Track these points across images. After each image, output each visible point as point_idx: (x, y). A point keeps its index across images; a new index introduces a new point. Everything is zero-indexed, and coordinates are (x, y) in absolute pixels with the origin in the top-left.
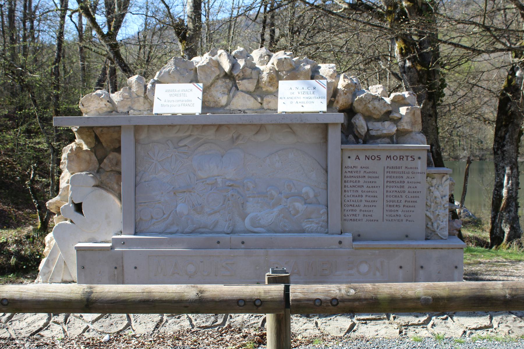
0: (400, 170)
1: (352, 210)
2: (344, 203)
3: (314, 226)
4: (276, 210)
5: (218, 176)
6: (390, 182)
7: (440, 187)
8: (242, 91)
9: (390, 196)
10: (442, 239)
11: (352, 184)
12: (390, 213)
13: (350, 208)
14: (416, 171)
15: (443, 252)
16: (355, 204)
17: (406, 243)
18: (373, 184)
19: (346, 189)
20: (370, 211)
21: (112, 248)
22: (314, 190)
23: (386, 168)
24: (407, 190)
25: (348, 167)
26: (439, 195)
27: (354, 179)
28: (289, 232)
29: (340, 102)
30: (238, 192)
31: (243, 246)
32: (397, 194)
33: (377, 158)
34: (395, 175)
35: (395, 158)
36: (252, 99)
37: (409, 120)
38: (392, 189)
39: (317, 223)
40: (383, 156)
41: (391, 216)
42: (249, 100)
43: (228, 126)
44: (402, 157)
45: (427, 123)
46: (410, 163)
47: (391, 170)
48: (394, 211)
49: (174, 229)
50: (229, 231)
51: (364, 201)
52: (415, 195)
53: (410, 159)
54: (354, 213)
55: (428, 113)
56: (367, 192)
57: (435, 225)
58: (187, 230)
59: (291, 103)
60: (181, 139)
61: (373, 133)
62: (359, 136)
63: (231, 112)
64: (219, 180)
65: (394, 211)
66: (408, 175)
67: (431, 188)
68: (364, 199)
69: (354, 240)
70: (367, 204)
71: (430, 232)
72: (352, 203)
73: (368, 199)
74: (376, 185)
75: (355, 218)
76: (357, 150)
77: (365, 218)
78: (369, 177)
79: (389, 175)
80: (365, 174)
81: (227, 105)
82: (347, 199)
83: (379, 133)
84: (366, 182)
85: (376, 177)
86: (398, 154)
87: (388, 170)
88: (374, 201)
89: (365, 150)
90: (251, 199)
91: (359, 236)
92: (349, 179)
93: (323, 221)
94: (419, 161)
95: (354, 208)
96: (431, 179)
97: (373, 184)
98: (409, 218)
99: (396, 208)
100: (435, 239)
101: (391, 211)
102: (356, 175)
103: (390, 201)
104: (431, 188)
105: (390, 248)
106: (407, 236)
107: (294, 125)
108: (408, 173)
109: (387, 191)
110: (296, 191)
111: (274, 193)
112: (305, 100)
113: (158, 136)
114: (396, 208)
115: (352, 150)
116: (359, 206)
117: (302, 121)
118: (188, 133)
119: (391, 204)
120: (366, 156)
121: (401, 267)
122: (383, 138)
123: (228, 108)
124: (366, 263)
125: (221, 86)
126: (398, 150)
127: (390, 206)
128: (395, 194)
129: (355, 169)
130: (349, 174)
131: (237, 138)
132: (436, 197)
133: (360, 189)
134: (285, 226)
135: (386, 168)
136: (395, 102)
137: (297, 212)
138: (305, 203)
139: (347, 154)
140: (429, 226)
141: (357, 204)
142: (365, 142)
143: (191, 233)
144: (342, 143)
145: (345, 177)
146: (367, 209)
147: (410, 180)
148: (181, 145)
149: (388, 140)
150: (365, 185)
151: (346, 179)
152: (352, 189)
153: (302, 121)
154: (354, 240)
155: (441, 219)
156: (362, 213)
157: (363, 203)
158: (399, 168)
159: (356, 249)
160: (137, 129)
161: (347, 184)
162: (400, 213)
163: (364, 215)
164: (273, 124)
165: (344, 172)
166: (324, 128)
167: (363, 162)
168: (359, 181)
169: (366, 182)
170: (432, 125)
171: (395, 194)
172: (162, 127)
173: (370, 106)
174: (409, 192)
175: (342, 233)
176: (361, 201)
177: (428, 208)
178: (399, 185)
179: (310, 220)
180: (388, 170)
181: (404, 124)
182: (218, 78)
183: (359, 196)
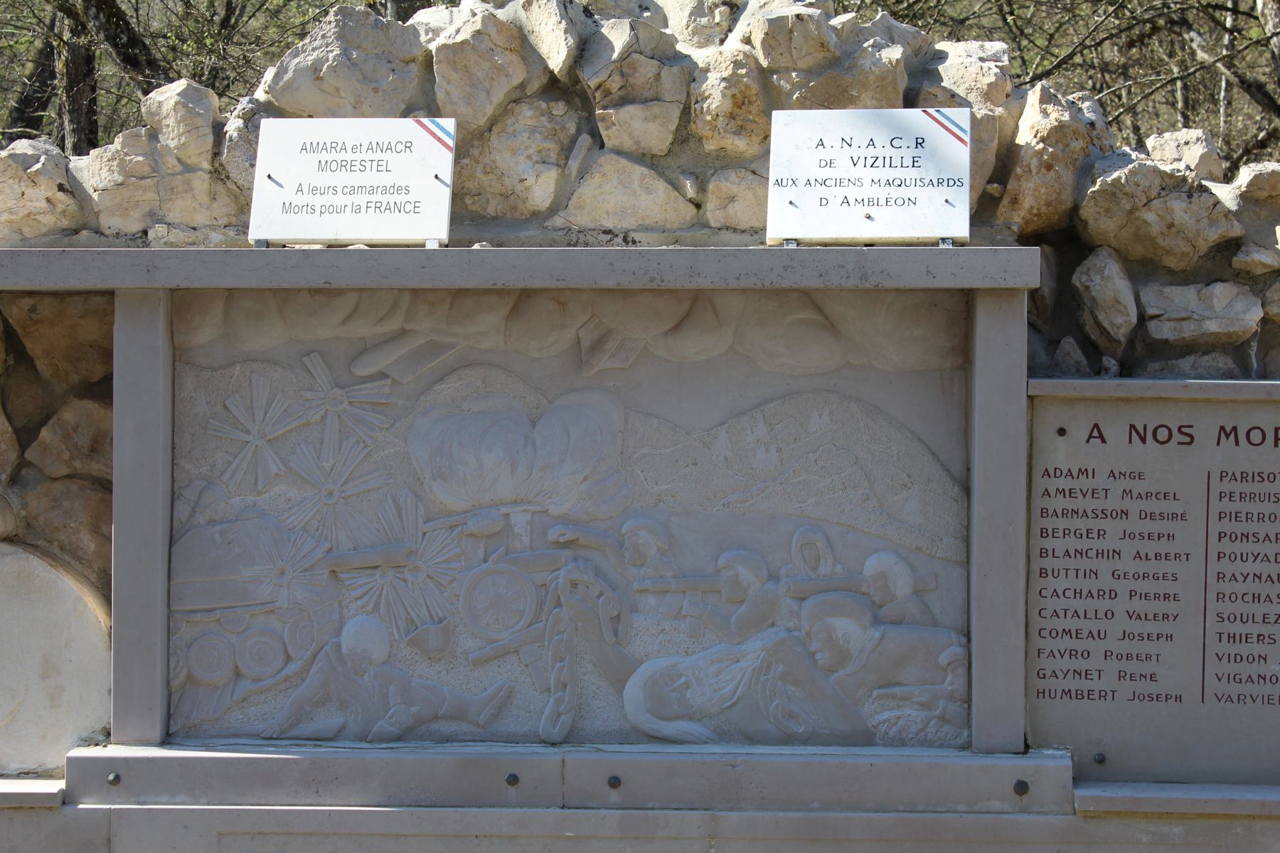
1: (1073, 654)
2: (1037, 623)
3: (912, 716)
4: (755, 648)
5: (515, 502)
6: (1233, 538)
8: (619, 152)
9: (1233, 598)
11: (1072, 543)
12: (1232, 668)
13: (1065, 643)
16: (1085, 626)
18: (1163, 547)
19: (1049, 563)
20: (1149, 657)
21: (66, 799)
22: (913, 569)
25: (1057, 473)
27: (1082, 524)
28: (807, 740)
29: (1027, 202)
30: (598, 573)
31: (614, 796)
33: (1177, 437)
34: (1255, 508)
36: (661, 186)
38: (1240, 567)
39: (922, 705)
40: (1205, 428)
41: (1236, 679)
42: (649, 190)
43: (560, 297)
47: (1238, 487)
48: (1251, 659)
49: (328, 720)
50: (557, 732)
51: (1120, 615)
54: (1081, 664)
56: (1136, 577)
58: (383, 726)
59: (823, 202)
60: (363, 350)
61: (1162, 331)
62: (1102, 343)
63: (575, 237)
64: (520, 520)
65: (1251, 659)
68: (1121, 605)
69: (1079, 778)
70: (1135, 627)
72: (1071, 624)
73: (1138, 605)
74: (1172, 548)
75: (1085, 685)
76: (1097, 401)
77: (1126, 688)
78: (1143, 515)
79: (1227, 506)
80: (1127, 504)
81: (553, 210)
82: (1052, 604)
83: (1189, 330)
84: (1132, 536)
85: (1174, 516)
87: (1227, 486)
88: (1165, 617)
90: (652, 600)
91: (1101, 760)
92: (1061, 523)
93: (951, 697)
95: (1079, 645)
97: (1163, 547)
101: (1238, 658)
102: (1089, 504)
103: (1233, 618)
105: (1233, 816)
107: (833, 290)
109: (1220, 576)
110: (839, 569)
111: (746, 575)
112: (881, 193)
113: (267, 337)
115: (1071, 401)
116: (1101, 635)
117: (864, 277)
118: (392, 325)
119: (1238, 628)
120: (1132, 426)
122: (1205, 353)
123: (558, 221)
125: (533, 131)
126: (1266, 402)
127: (1232, 638)
128: (1252, 587)
129: (1085, 483)
130: (1059, 503)
131: (597, 345)
133: (1104, 567)
134: (791, 716)
136: (1257, 202)
137: (843, 657)
138: (877, 621)
139: (1051, 417)
141: (1094, 626)
142: (1127, 370)
143: (399, 738)
144: (1033, 371)
146: (1133, 647)
148: (362, 370)
149: (1224, 362)
150: (1128, 548)
151: (1049, 523)
152: (1071, 563)
153: (864, 277)
154: (1079, 778)
156: (1114, 666)
157: (1121, 623)
159: (1088, 816)
160: (182, 304)
161: (1049, 543)
163: (1121, 675)
166: (960, 308)
167: (1120, 451)
168: (1101, 534)
169: (1132, 536)
171: (1252, 587)
172: (283, 297)
173: (1150, 217)
176: (1110, 615)
179: (897, 690)
180: (1227, 486)
182: (518, 97)
183: (1101, 594)
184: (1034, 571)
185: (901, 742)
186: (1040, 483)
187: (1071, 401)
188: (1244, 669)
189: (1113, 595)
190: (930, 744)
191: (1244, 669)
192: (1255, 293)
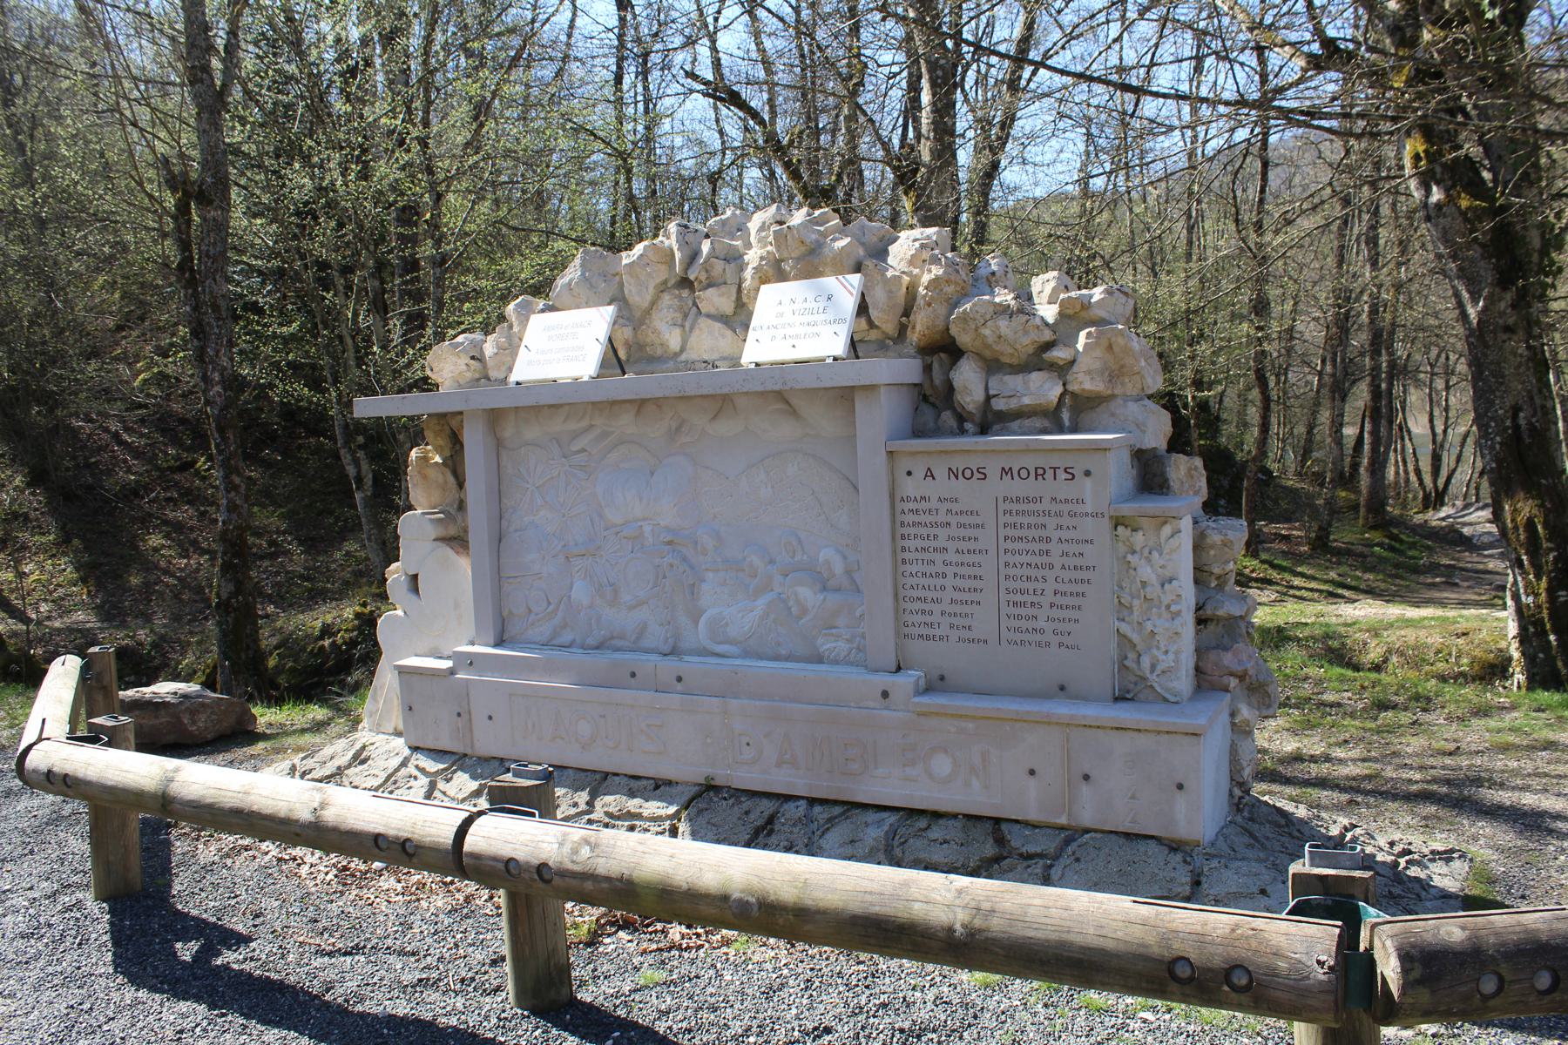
0: (1038, 507)
1: (923, 612)
2: (902, 593)
3: (842, 647)
4: (761, 603)
5: (644, 519)
6: (1013, 539)
7: (1155, 554)
8: (709, 316)
9: (1015, 578)
10: (1165, 700)
11: (919, 543)
12: (1017, 624)
13: (918, 605)
14: (1079, 508)
15: (1142, 740)
16: (930, 595)
17: (1062, 709)
18: (971, 545)
19: (907, 555)
21: (452, 671)
22: (845, 558)
23: (1000, 500)
24: (1058, 564)
25: (908, 499)
26: (1154, 577)
27: (924, 531)
28: (788, 659)
29: (918, 327)
30: (685, 559)
31: (679, 687)
32: (1033, 572)
33: (977, 475)
34: (1026, 520)
35: (1024, 473)
36: (729, 333)
37: (1098, 365)
38: (1018, 559)
40: (993, 471)
41: (1018, 630)
42: (723, 336)
43: (658, 402)
44: (1040, 471)
45: (1501, 349)
46: (1060, 487)
47: (1015, 507)
48: (1028, 618)
49: (566, 637)
50: (666, 649)
51: (949, 589)
52: (1079, 575)
53: (1062, 475)
54: (928, 619)
55: (1501, 322)
56: (957, 564)
57: (1146, 662)
58: (591, 641)
59: (773, 338)
60: (575, 435)
61: (999, 405)
63: (690, 365)
64: (647, 529)
65: (1028, 618)
66: (1060, 521)
67: (1130, 558)
68: (949, 582)
70: (958, 596)
71: (1133, 679)
72: (921, 594)
73: (959, 582)
75: (931, 632)
76: (929, 453)
77: (954, 635)
78: (960, 525)
80: (949, 518)
81: (683, 350)
83: (1013, 404)
84: (953, 539)
85: (977, 526)
86: (1031, 462)
87: (1008, 506)
89: (946, 452)
90: (710, 575)
91: (942, 678)
92: (912, 531)
94: (1088, 482)
96: (1128, 532)
97: (971, 545)
98: (1067, 640)
99: (1030, 611)
100: (1147, 701)
101: (1019, 617)
103: (1015, 591)
104: (1130, 558)
106: (1062, 688)
107: (783, 392)
108: (1060, 514)
109: (1007, 565)
111: (756, 561)
112: (802, 330)
113: (532, 432)
114: (1030, 611)
115: (913, 454)
116: (939, 601)
117: (785, 383)
118: (585, 423)
119: (1019, 598)
121: (1032, 772)
123: (683, 357)
124: (946, 751)
125: (670, 307)
127: (1015, 604)
128: (1027, 571)
129: (924, 505)
130: (910, 518)
131: (678, 429)
132: (1144, 584)
133: (938, 557)
134: (779, 644)
135: (1000, 500)
136: (1069, 317)
137: (804, 611)
138: (824, 589)
139: (904, 464)
140: (1127, 663)
141: (934, 595)
142: (984, 430)
143: (597, 648)
145: (902, 524)
146: (958, 609)
147: (1065, 535)
148: (574, 448)
150: (952, 546)
151: (906, 531)
152: (919, 556)
153: (785, 383)
155: (1162, 645)
156: (946, 620)
157: (949, 594)
158: (1035, 500)
159: (920, 714)
160: (494, 417)
161: (906, 543)
162: (1041, 624)
164: (746, 393)
165: (898, 510)
166: (846, 397)
167: (943, 485)
169: (953, 539)
170: (1515, 354)
171: (1027, 571)
172: (536, 410)
173: (986, 332)
174: (1063, 567)
175: (899, 669)
177: (1126, 612)
178: (1036, 547)
180: (1008, 506)
181: (1081, 377)
182: (663, 288)
184: (898, 561)
185: (836, 662)
186: (899, 506)
187: (913, 454)
188: (1023, 624)
189: (944, 576)
190: (851, 664)
191: (1023, 624)
192: (1060, 377)
